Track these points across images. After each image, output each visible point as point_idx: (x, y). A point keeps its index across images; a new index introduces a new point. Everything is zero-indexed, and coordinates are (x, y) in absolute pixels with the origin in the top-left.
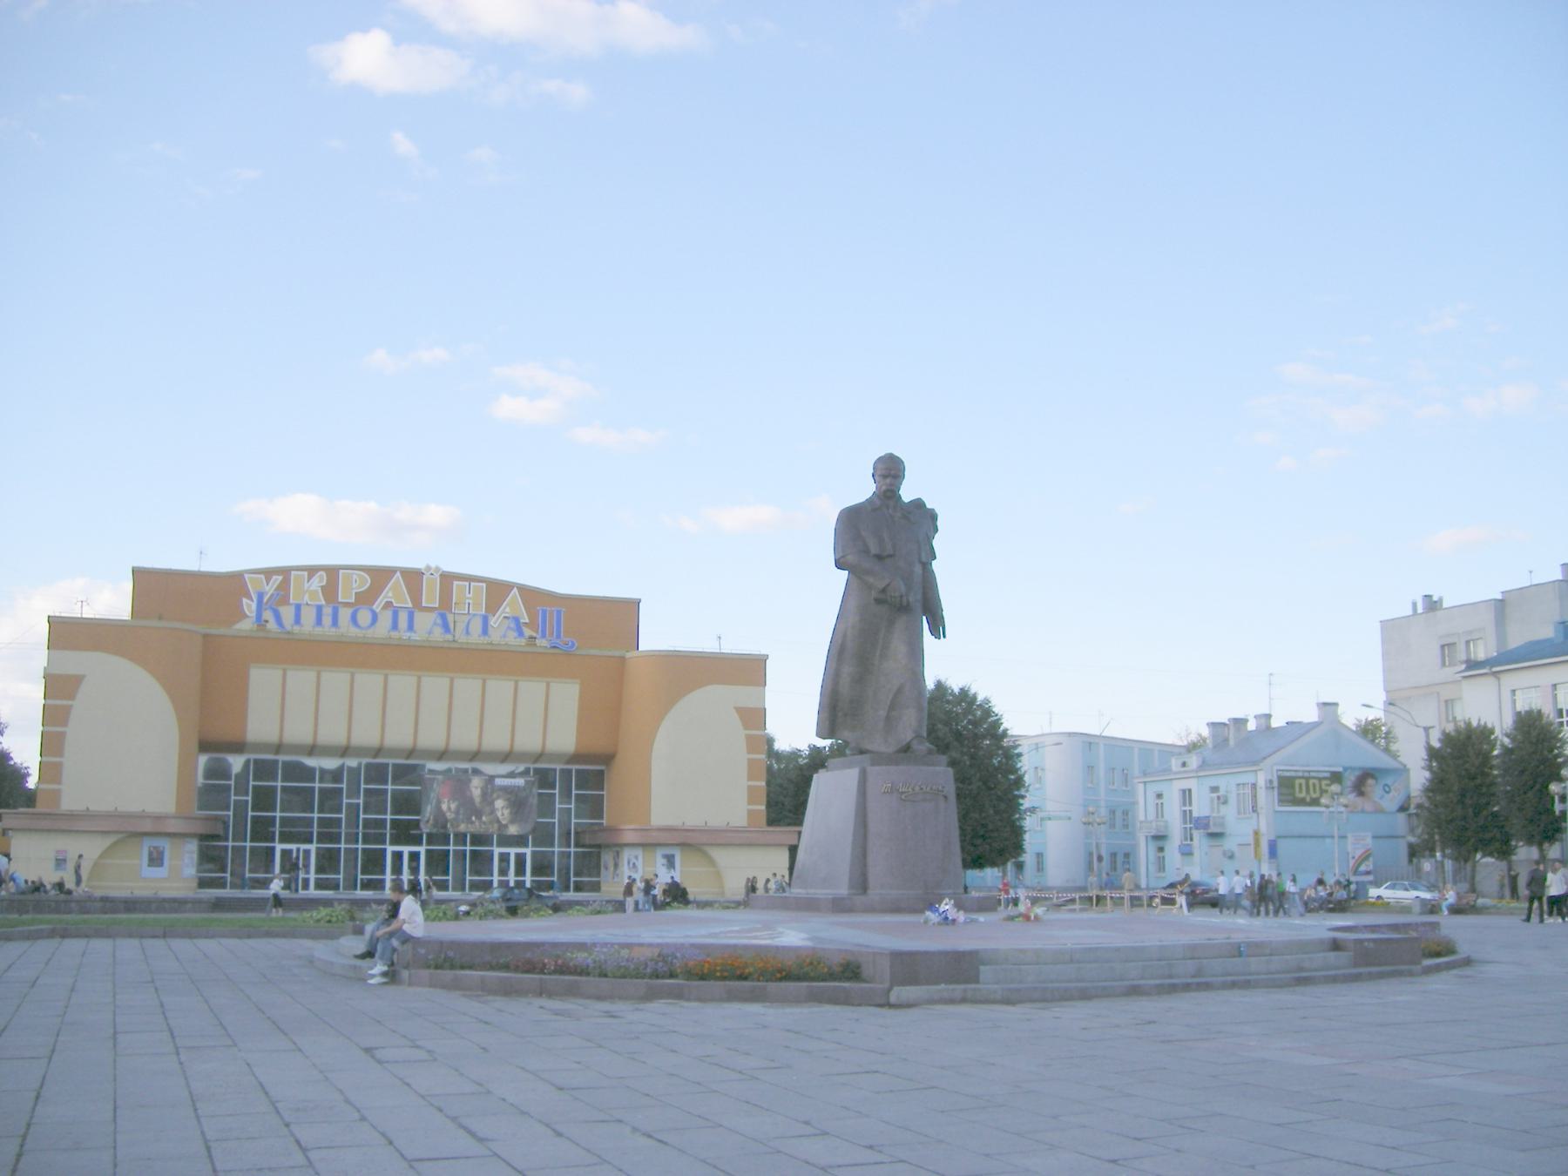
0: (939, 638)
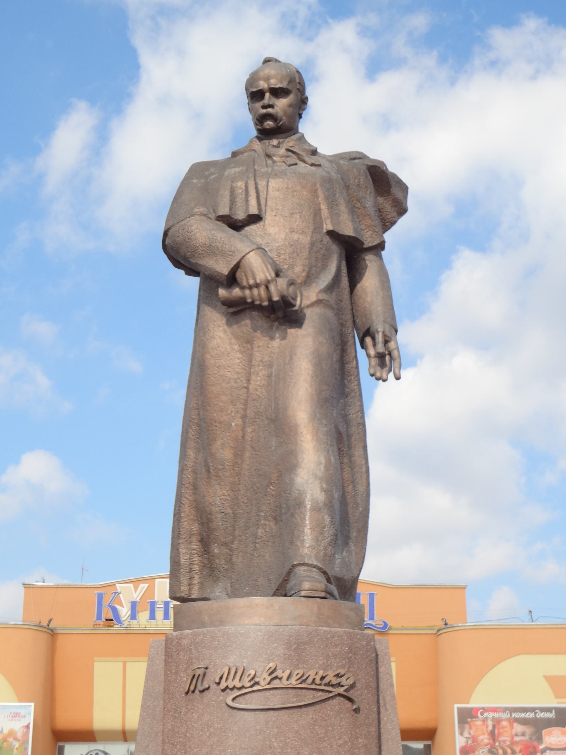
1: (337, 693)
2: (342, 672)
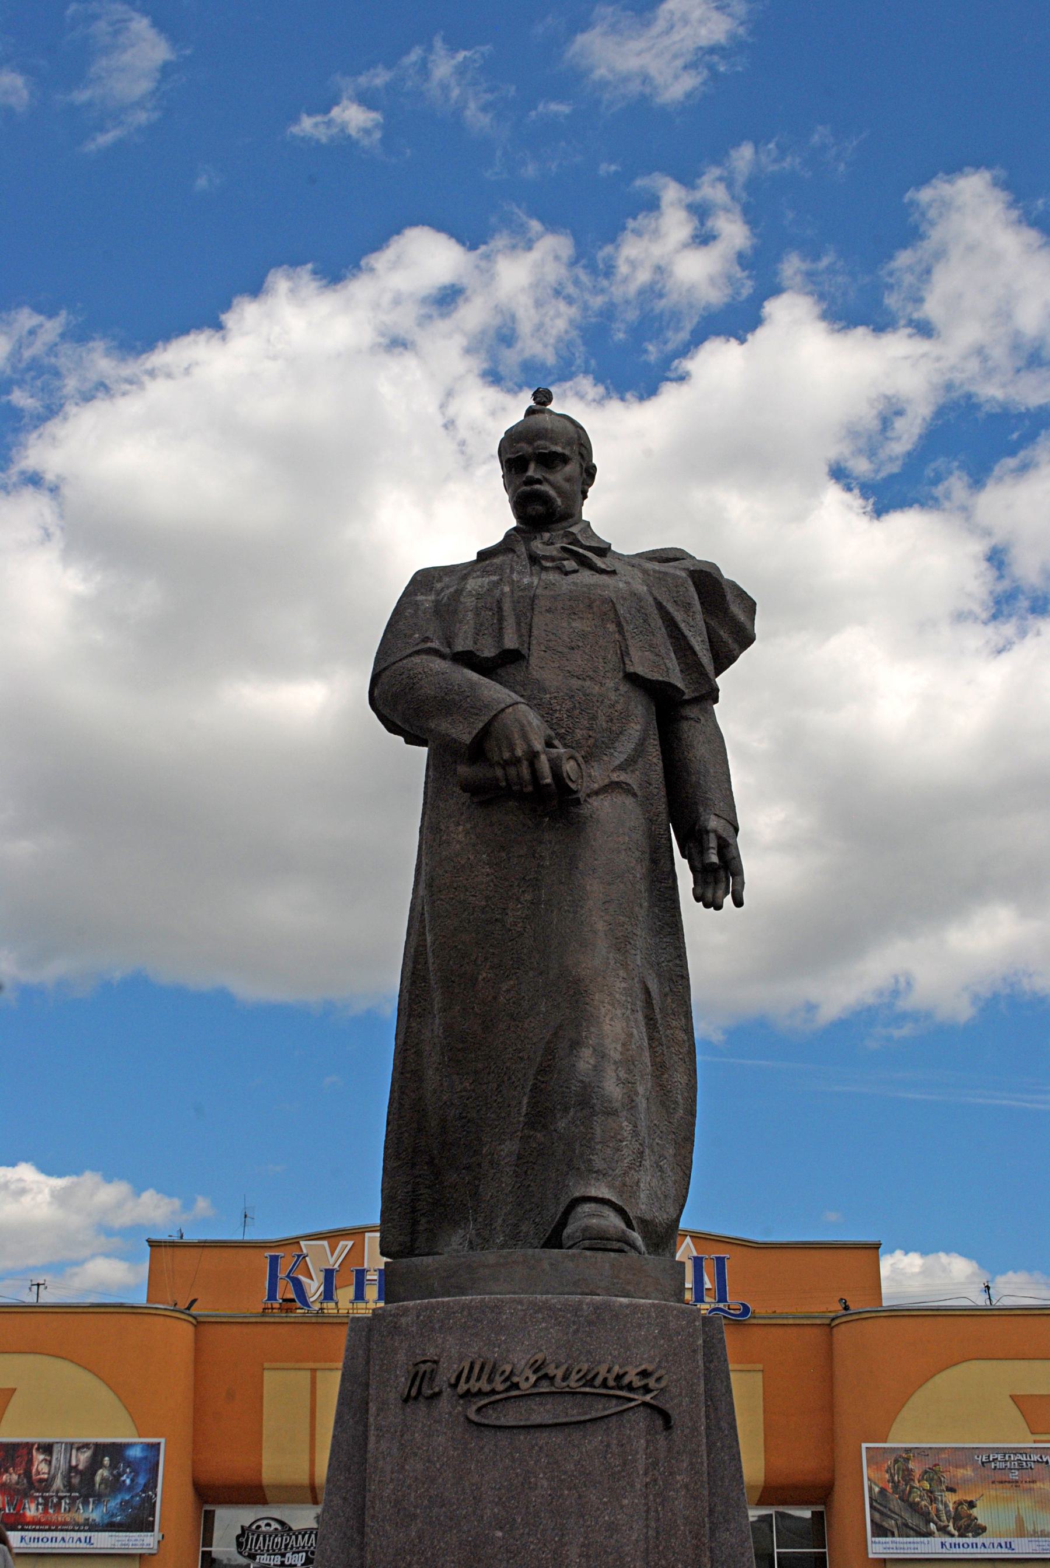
0: (718, 907)
1: (639, 1402)
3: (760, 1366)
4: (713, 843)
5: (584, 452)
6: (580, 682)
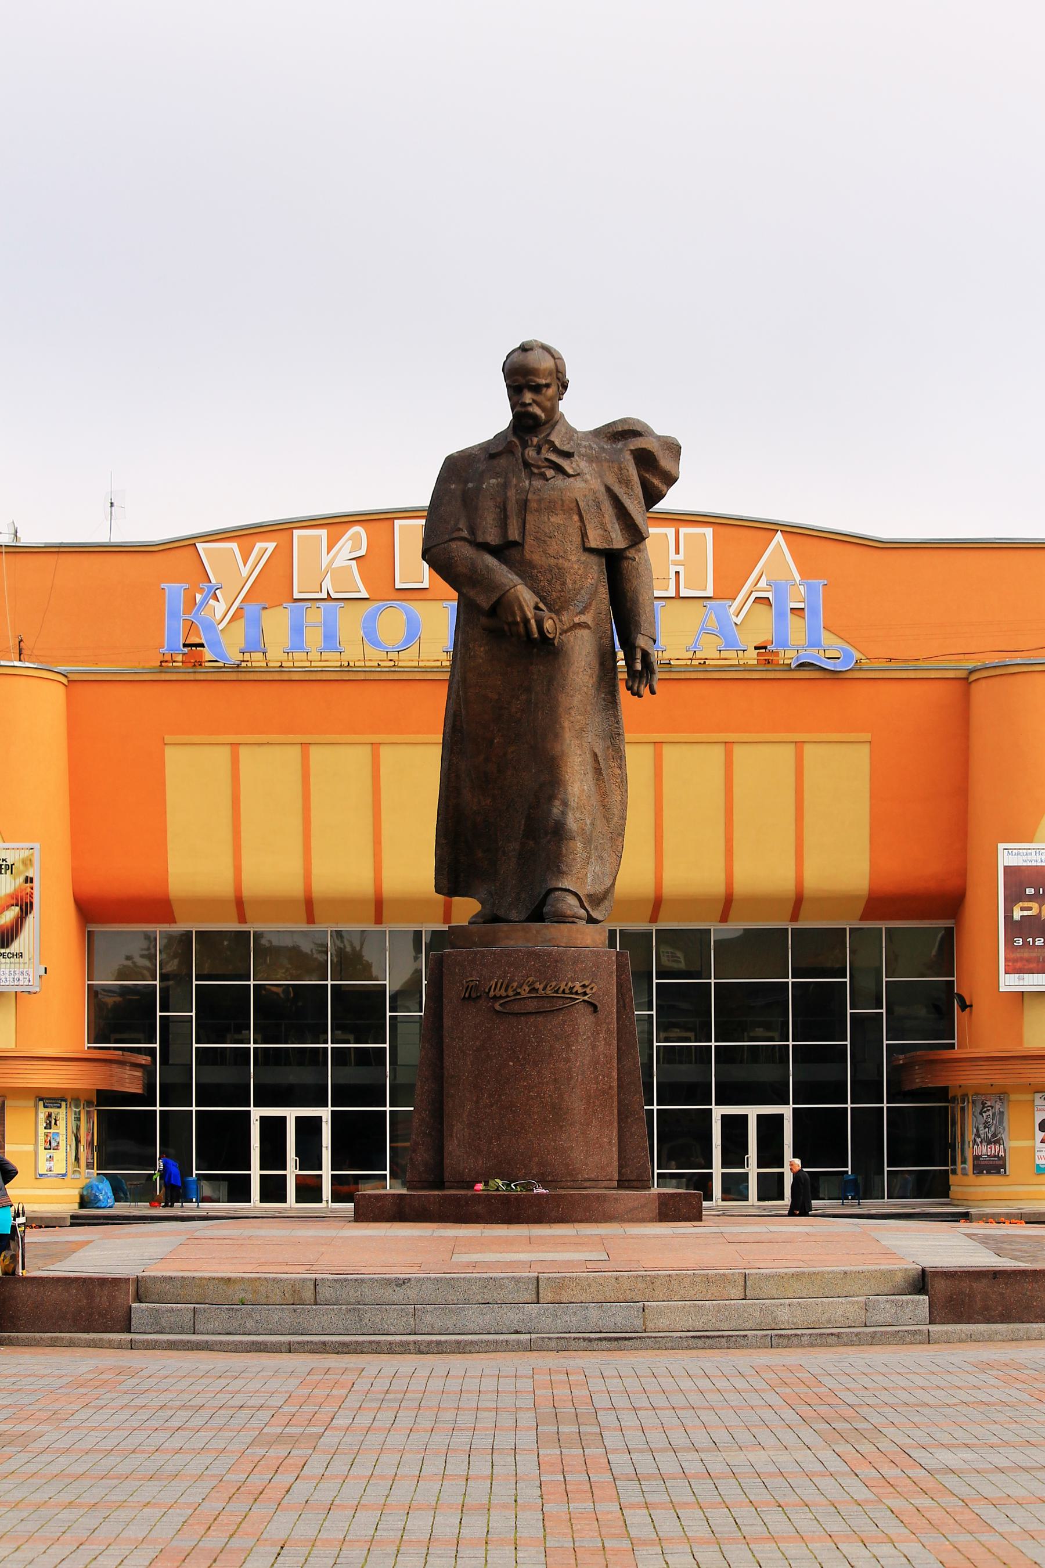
2: (587, 983)
3: (867, 737)
4: (639, 655)
5: (560, 375)
6: (556, 561)
